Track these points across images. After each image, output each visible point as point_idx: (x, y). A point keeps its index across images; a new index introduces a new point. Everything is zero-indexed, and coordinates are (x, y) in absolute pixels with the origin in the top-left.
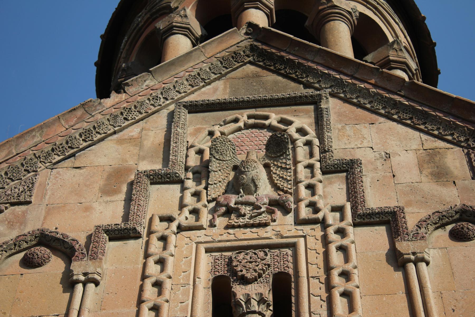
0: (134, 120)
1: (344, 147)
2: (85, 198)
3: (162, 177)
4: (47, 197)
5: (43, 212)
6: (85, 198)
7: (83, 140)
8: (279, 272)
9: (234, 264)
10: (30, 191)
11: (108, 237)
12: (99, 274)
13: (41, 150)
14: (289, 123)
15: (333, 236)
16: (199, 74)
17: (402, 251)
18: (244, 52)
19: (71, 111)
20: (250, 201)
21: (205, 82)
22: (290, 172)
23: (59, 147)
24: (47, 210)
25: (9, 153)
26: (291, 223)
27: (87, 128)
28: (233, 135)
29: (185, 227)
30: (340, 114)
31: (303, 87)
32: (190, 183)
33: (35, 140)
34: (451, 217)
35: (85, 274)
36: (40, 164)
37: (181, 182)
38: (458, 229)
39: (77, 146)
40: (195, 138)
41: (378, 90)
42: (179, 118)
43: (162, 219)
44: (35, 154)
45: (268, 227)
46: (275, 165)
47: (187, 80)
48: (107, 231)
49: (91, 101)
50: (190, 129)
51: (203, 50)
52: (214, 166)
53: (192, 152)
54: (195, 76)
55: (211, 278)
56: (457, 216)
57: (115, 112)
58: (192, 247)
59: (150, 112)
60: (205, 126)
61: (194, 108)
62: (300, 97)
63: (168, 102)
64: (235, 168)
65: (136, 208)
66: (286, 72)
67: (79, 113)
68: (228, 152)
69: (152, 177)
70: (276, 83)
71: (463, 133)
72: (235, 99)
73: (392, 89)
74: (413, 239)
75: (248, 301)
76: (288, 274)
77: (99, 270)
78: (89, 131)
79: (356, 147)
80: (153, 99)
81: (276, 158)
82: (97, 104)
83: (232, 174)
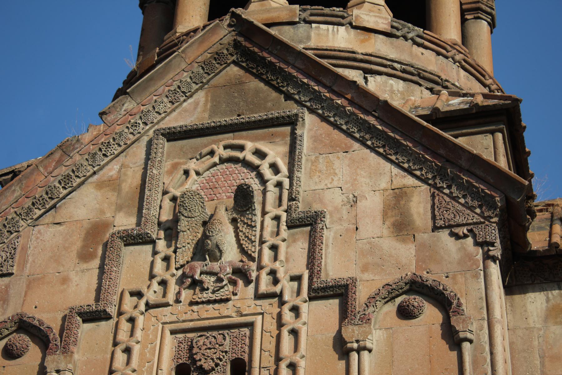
0: (113, 156)
1: (314, 188)
2: (63, 266)
3: (134, 238)
4: (28, 265)
5: (25, 286)
6: (63, 266)
7: (63, 187)
8: (236, 359)
10: (12, 259)
11: (81, 320)
13: (21, 207)
15: (288, 316)
16: (179, 87)
17: (346, 339)
18: (227, 50)
19: (49, 156)
20: (214, 271)
21: (186, 96)
22: (255, 231)
23: (39, 200)
24: (28, 283)
26: (250, 297)
27: (66, 174)
28: (208, 172)
29: (153, 305)
30: (315, 139)
31: (284, 97)
32: (161, 245)
33: (15, 195)
34: (401, 289)
36: (22, 222)
37: (153, 242)
38: (404, 306)
39: (57, 196)
40: (171, 178)
41: (354, 109)
42: (155, 153)
43: (132, 294)
44: (16, 212)
45: (230, 302)
46: (241, 221)
47: (167, 96)
48: (80, 314)
49: (68, 140)
50: (167, 165)
51: (183, 55)
52: (183, 224)
53: (167, 198)
54: (175, 90)
55: (174, 366)
56: (408, 287)
57: (93, 149)
58: (158, 330)
59: (129, 142)
60: (182, 161)
61: (173, 135)
62: (277, 118)
63: (147, 127)
65: (107, 283)
66: (268, 77)
67: (57, 156)
68: (197, 207)
69: (125, 239)
70: (257, 91)
71: (431, 169)
72: (213, 124)
73: (368, 108)
74: (360, 322)
76: (243, 360)
77: (70, 366)
78: (68, 176)
79: (326, 187)
80: (132, 126)
82: (75, 141)
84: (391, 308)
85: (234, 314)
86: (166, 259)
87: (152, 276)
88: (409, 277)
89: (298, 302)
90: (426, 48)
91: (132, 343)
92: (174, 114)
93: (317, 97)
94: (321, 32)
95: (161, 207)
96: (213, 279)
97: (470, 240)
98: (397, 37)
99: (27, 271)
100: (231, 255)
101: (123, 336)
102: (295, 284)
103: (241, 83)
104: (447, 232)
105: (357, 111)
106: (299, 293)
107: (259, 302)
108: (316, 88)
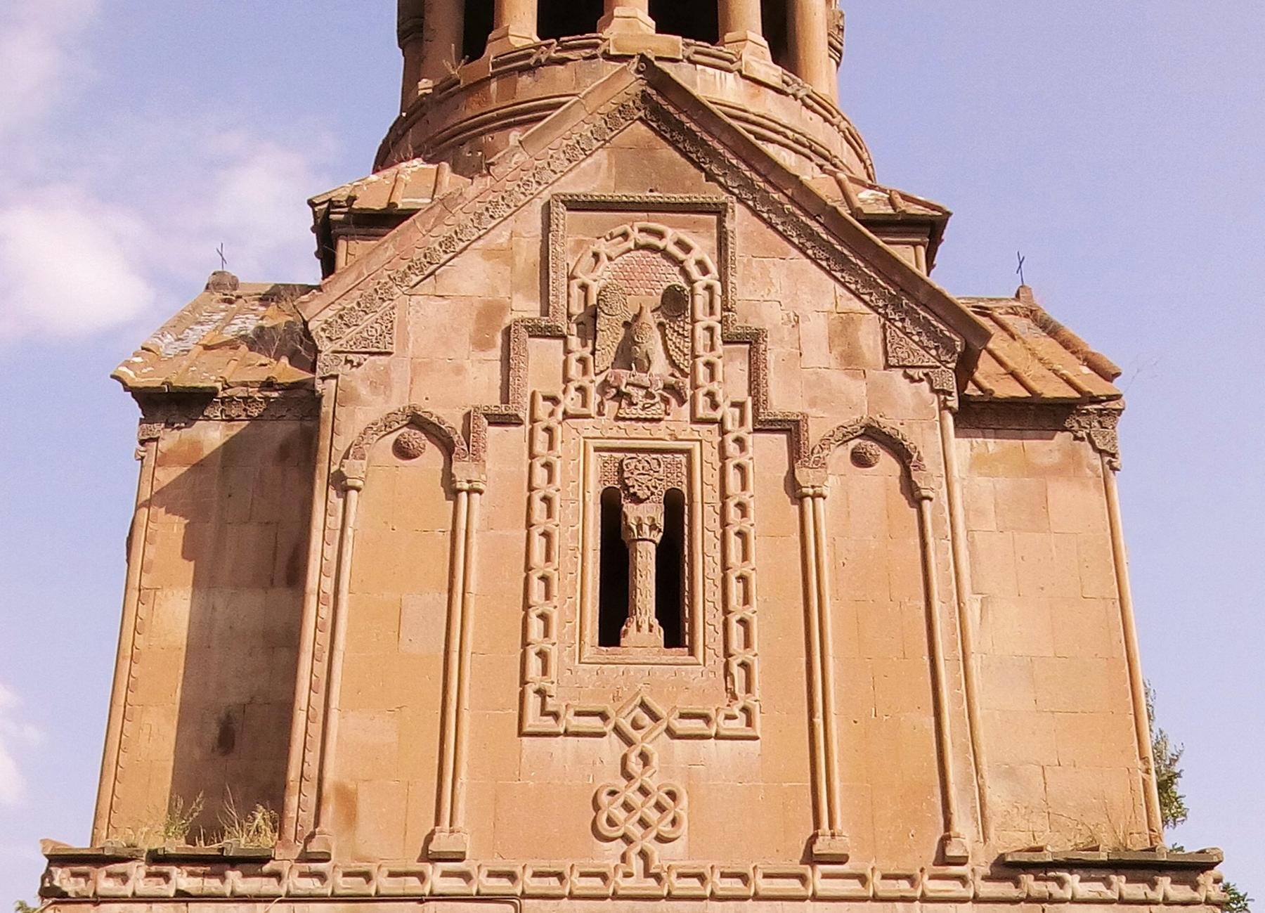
4: (410, 345)
9: (626, 475)
11: (486, 422)
12: (484, 482)
14: (687, 249)
15: (732, 448)
30: (747, 237)
32: (574, 342)
35: (469, 482)
43: (546, 398)
48: (486, 415)
50: (570, 241)
52: (602, 323)
55: (601, 490)
59: (520, 204)
61: (575, 205)
63: (541, 188)
64: (626, 324)
67: (437, 210)
70: (673, 163)
71: (882, 296)
75: (639, 526)
77: (483, 477)
83: (622, 330)
84: (844, 452)
85: (667, 438)
86: (582, 360)
87: (566, 380)
88: (864, 421)
89: (742, 433)
90: (815, 111)
91: (553, 459)
92: (571, 175)
93: (749, 185)
94: (708, 78)
95: (569, 295)
96: (642, 392)
97: (925, 385)
98: (787, 94)
99: (410, 353)
102: (737, 411)
104: (901, 371)
105: (798, 212)
106: (742, 422)
107: (695, 427)
108: (748, 173)
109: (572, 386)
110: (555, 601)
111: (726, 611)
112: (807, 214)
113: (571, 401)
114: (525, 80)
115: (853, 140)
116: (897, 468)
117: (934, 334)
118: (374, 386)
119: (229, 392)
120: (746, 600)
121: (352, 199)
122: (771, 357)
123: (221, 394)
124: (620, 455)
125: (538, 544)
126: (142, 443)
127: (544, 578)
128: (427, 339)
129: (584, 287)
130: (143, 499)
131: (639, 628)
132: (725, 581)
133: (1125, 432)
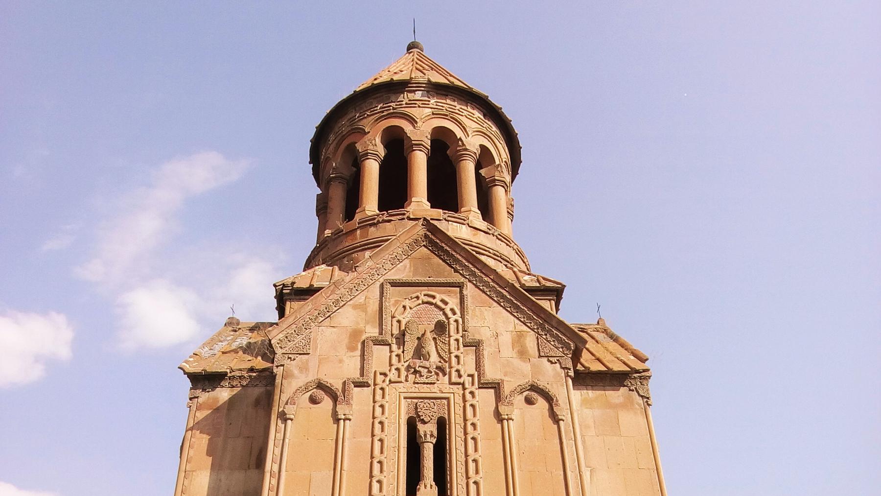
14: (446, 303)
25: (296, 317)
30: (473, 297)
32: (394, 347)
37: (390, 345)
43: (381, 374)
48: (353, 383)
50: (392, 301)
52: (407, 338)
61: (394, 284)
64: (418, 338)
67: (332, 288)
70: (439, 265)
71: (536, 324)
75: (425, 435)
81: (440, 335)
84: (522, 398)
86: (398, 356)
89: (473, 389)
91: (384, 403)
93: (473, 274)
96: (426, 370)
97: (558, 365)
100: (434, 358)
101: (378, 397)
103: (429, 258)
106: (473, 384)
109: (393, 368)
110: (385, 474)
111: (468, 478)
112: (501, 287)
113: (393, 375)
114: (372, 229)
115: (519, 253)
116: (546, 405)
117: (560, 341)
118: (301, 369)
119: (233, 374)
120: (477, 472)
121: (293, 283)
122: (485, 353)
123: (229, 375)
124: (416, 401)
125: (377, 445)
126: (191, 399)
127: (380, 462)
128: (326, 348)
129: (399, 322)
130: (189, 426)
131: (425, 487)
132: (466, 462)
133: (652, 386)
